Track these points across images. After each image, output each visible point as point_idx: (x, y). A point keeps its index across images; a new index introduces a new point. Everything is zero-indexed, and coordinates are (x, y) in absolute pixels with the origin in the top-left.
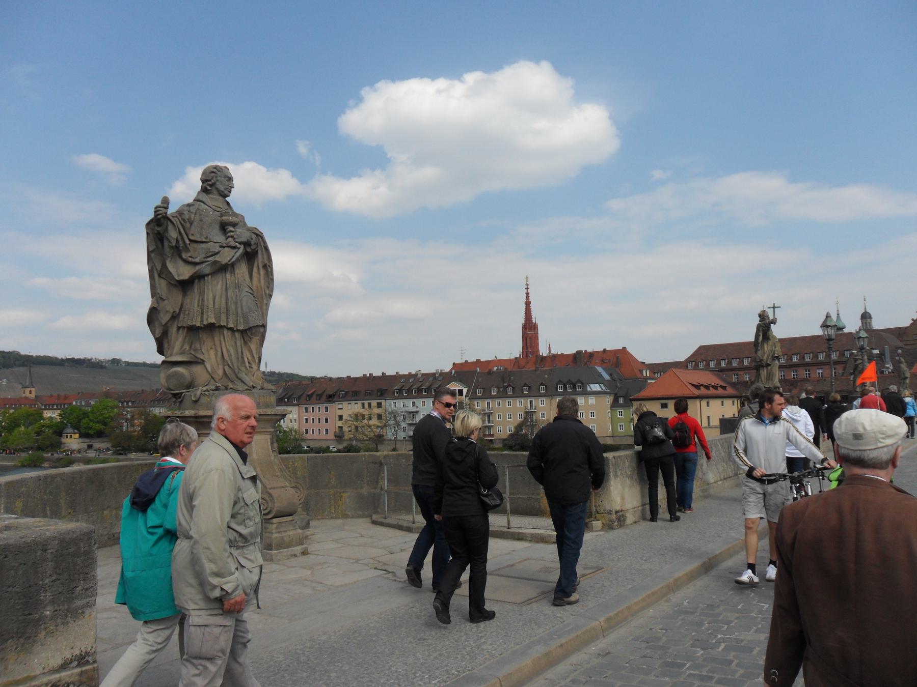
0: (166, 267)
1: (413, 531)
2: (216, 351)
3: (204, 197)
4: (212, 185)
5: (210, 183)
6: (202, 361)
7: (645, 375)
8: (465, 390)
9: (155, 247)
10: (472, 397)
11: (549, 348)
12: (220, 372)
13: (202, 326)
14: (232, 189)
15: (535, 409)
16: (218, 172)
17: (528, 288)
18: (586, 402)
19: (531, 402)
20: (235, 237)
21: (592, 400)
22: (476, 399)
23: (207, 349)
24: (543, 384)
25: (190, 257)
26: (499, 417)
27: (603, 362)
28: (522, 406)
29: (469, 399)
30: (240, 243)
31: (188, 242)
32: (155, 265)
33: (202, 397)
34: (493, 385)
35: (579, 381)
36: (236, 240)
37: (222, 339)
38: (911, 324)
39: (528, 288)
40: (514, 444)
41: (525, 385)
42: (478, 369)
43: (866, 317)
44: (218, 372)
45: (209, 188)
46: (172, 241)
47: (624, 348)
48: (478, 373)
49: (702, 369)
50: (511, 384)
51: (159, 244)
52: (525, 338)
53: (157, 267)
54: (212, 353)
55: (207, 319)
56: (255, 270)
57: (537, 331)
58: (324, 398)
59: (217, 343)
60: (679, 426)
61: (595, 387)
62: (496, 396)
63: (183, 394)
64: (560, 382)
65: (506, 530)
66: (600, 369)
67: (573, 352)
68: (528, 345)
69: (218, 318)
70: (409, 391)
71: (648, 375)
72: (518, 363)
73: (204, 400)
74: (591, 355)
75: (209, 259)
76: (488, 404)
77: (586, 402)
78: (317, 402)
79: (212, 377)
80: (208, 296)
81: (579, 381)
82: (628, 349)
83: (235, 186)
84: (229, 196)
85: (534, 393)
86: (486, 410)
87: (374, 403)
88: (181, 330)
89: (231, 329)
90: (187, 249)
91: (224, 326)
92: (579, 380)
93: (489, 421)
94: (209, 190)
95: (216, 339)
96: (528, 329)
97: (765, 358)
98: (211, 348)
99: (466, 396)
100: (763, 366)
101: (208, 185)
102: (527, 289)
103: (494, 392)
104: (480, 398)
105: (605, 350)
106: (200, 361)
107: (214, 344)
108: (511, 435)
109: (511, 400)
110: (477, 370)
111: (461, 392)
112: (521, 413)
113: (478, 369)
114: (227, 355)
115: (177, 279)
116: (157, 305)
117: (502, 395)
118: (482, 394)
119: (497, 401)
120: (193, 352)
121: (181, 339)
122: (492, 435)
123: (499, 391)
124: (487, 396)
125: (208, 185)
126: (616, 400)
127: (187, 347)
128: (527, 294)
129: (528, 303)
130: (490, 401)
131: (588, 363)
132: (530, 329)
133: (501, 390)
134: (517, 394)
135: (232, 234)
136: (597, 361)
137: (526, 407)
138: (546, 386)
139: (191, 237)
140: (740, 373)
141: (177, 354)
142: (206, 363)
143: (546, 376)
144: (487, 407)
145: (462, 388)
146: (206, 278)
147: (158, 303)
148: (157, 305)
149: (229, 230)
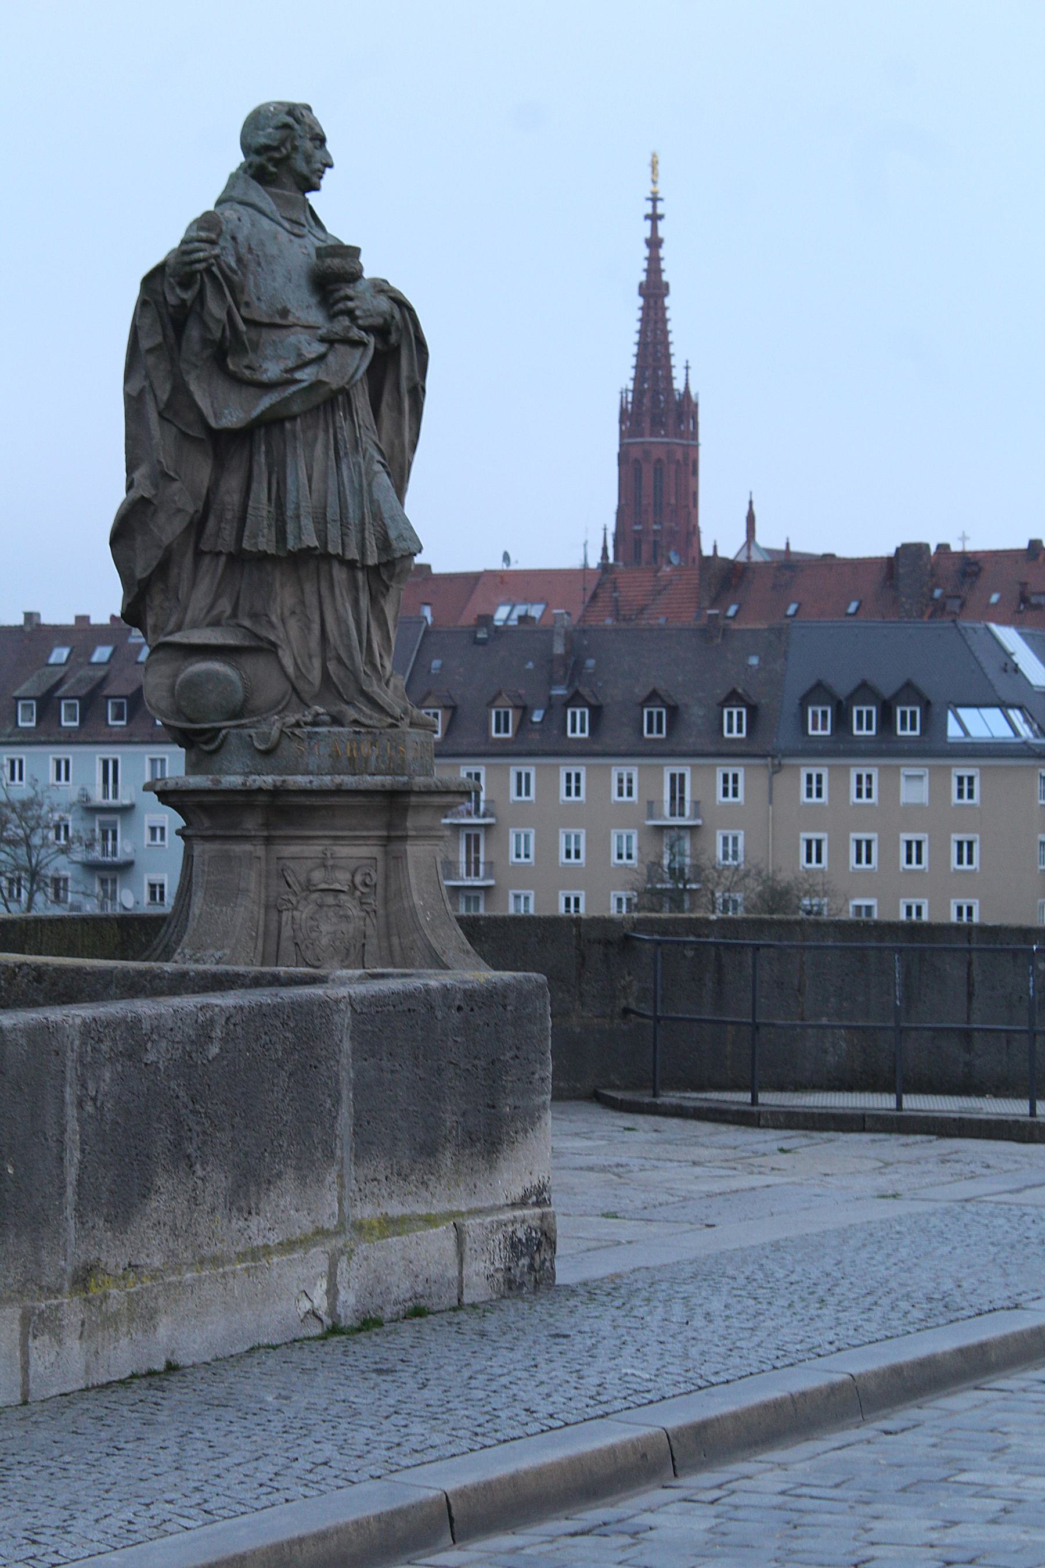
0: (189, 395)
1: (762, 1122)
3: (258, 195)
4: (277, 163)
5: (277, 155)
6: (269, 647)
9: (159, 339)
11: (751, 519)
12: (316, 676)
13: (282, 554)
14: (328, 170)
16: (297, 126)
17: (661, 217)
20: (358, 313)
23: (282, 614)
24: (733, 698)
25: (248, 367)
30: (366, 329)
31: (242, 327)
32: (151, 385)
33: (285, 742)
36: (360, 322)
37: (325, 592)
39: (661, 217)
42: (427, 612)
44: (310, 678)
45: (273, 169)
46: (212, 325)
51: (170, 332)
53: (159, 393)
54: (293, 624)
55: (299, 538)
56: (387, 398)
57: (695, 435)
59: (311, 599)
63: (224, 732)
64: (818, 692)
65: (1030, 1119)
66: (1009, 637)
67: (887, 550)
69: (322, 536)
73: (290, 748)
75: (298, 375)
79: (294, 689)
80: (297, 474)
81: (910, 692)
83: (335, 160)
84: (316, 188)
88: (207, 560)
89: (351, 565)
91: (337, 557)
92: (909, 685)
94: (272, 174)
95: (309, 588)
98: (293, 613)
101: (270, 159)
102: (654, 218)
106: (266, 645)
107: (302, 602)
109: (579, 767)
113: (427, 612)
114: (336, 633)
115: (213, 423)
116: (153, 492)
119: (515, 768)
120: (247, 623)
125: (270, 159)
128: (654, 243)
132: (657, 423)
133: (537, 717)
135: (350, 304)
137: (650, 803)
139: (244, 312)
141: (195, 625)
142: (280, 652)
143: (754, 661)
146: (288, 425)
147: (156, 486)
148: (153, 492)
149: (342, 293)
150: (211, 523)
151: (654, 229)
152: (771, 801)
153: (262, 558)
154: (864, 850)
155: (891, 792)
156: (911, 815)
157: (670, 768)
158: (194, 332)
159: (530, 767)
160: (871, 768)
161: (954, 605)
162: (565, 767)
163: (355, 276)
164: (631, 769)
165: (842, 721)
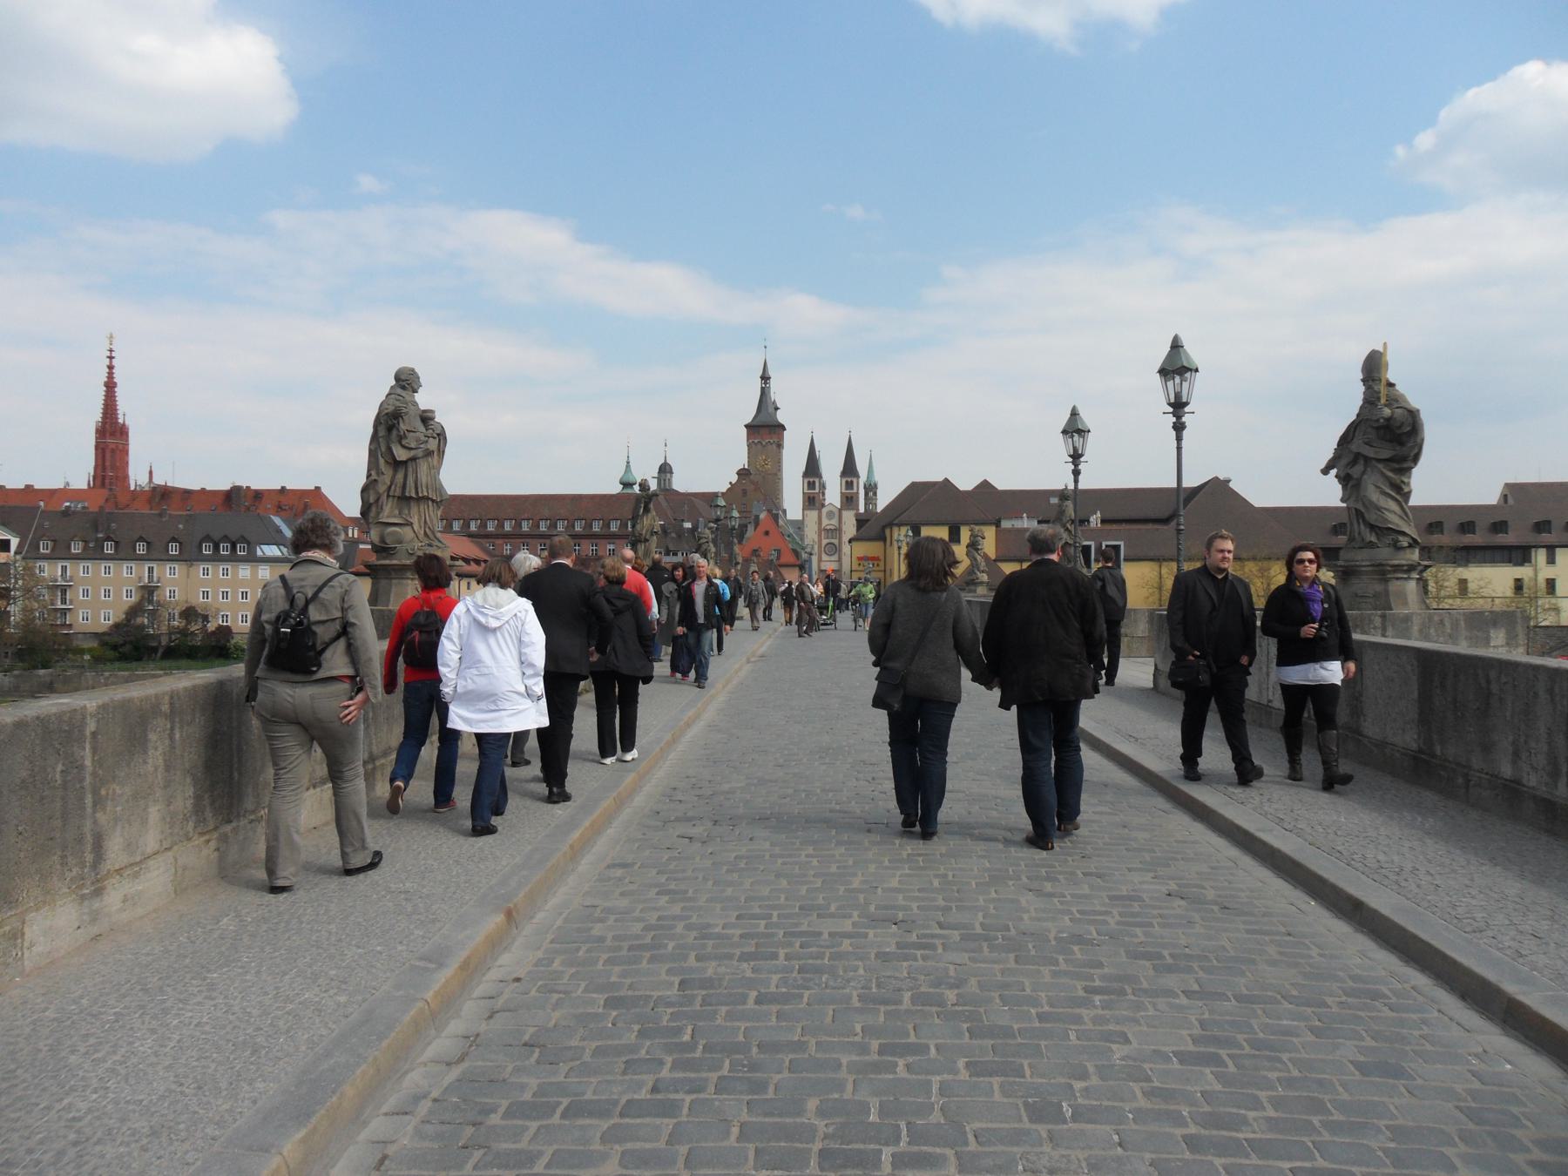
2: (420, 515)
7: (350, 535)
8: (14, 542)
10: (29, 555)
11: (151, 473)
15: (158, 582)
18: (254, 574)
19: (151, 570)
22: (168, 560)
24: (174, 540)
26: (86, 593)
27: (279, 509)
28: (133, 575)
29: (24, 558)
34: (75, 536)
35: (243, 539)
38: (729, 489)
40: (121, 642)
41: (141, 539)
42: (42, 504)
43: (665, 470)
47: (318, 488)
48: (43, 512)
49: (456, 532)
50: (112, 536)
52: (101, 450)
57: (127, 440)
60: (422, 619)
61: (272, 551)
62: (81, 556)
64: (207, 538)
66: (277, 521)
67: (226, 486)
68: (108, 464)
71: (356, 536)
72: (115, 497)
74: (258, 495)
76: (64, 569)
77: (254, 574)
81: (243, 539)
82: (324, 490)
85: (157, 553)
86: (60, 579)
88: (391, 499)
90: (405, 437)
92: (243, 537)
93: (64, 601)
95: (422, 507)
96: (108, 435)
97: (644, 532)
99: (16, 553)
100: (641, 542)
102: (111, 358)
103: (76, 548)
105: (283, 488)
108: (117, 626)
109: (111, 564)
110: (39, 507)
112: (129, 588)
117: (94, 553)
118: (53, 550)
119: (82, 565)
121: (390, 505)
122: (70, 626)
123: (85, 548)
127: (397, 512)
128: (111, 367)
129: (110, 386)
130: (67, 563)
131: (253, 508)
132: (113, 434)
134: (124, 553)
136: (269, 506)
137: (140, 578)
138: (180, 543)
140: (499, 541)
143: (181, 526)
144: (60, 573)
145: (9, 537)
150: (393, 487)
151: (111, 362)
152: (188, 577)
153: (411, 498)
154: (225, 595)
155: (235, 574)
156: (243, 583)
158: (394, 432)
159: (89, 564)
160: (229, 566)
161: (253, 508)
162: (103, 564)
163: (433, 419)
164: (133, 564)
165: (216, 548)
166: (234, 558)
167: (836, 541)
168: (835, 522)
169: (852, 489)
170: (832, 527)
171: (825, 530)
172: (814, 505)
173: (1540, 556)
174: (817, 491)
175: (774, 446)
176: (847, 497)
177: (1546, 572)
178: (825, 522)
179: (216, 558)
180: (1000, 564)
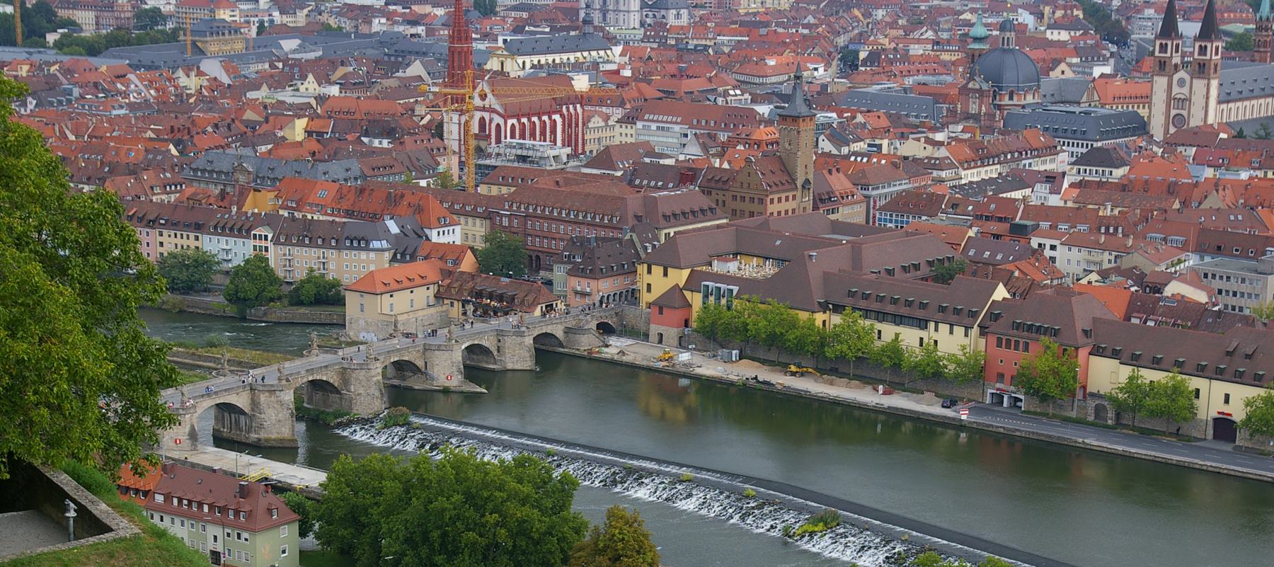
8: (270, 236)
18: (368, 257)
21: (372, 255)
58: (145, 222)
64: (347, 238)
70: (223, 228)
77: (368, 257)
78: (139, 224)
87: (192, 235)
104: (282, 244)
109: (307, 249)
111: (266, 237)
117: (301, 244)
119: (296, 248)
124: (288, 242)
126: (395, 255)
130: (290, 247)
134: (313, 244)
155: (360, 257)
156: (363, 261)
157: (322, 250)
159: (299, 248)
160: (356, 252)
162: (305, 249)
165: (352, 243)
166: (359, 248)
167: (1185, 113)
168: (1185, 90)
169: (1205, 55)
170: (1183, 97)
171: (1175, 99)
172: (1164, 70)
173: (932, 325)
174: (1169, 55)
175: (796, 132)
176: (1199, 64)
177: (935, 336)
178: (1176, 89)
179: (351, 248)
180: (685, 292)
